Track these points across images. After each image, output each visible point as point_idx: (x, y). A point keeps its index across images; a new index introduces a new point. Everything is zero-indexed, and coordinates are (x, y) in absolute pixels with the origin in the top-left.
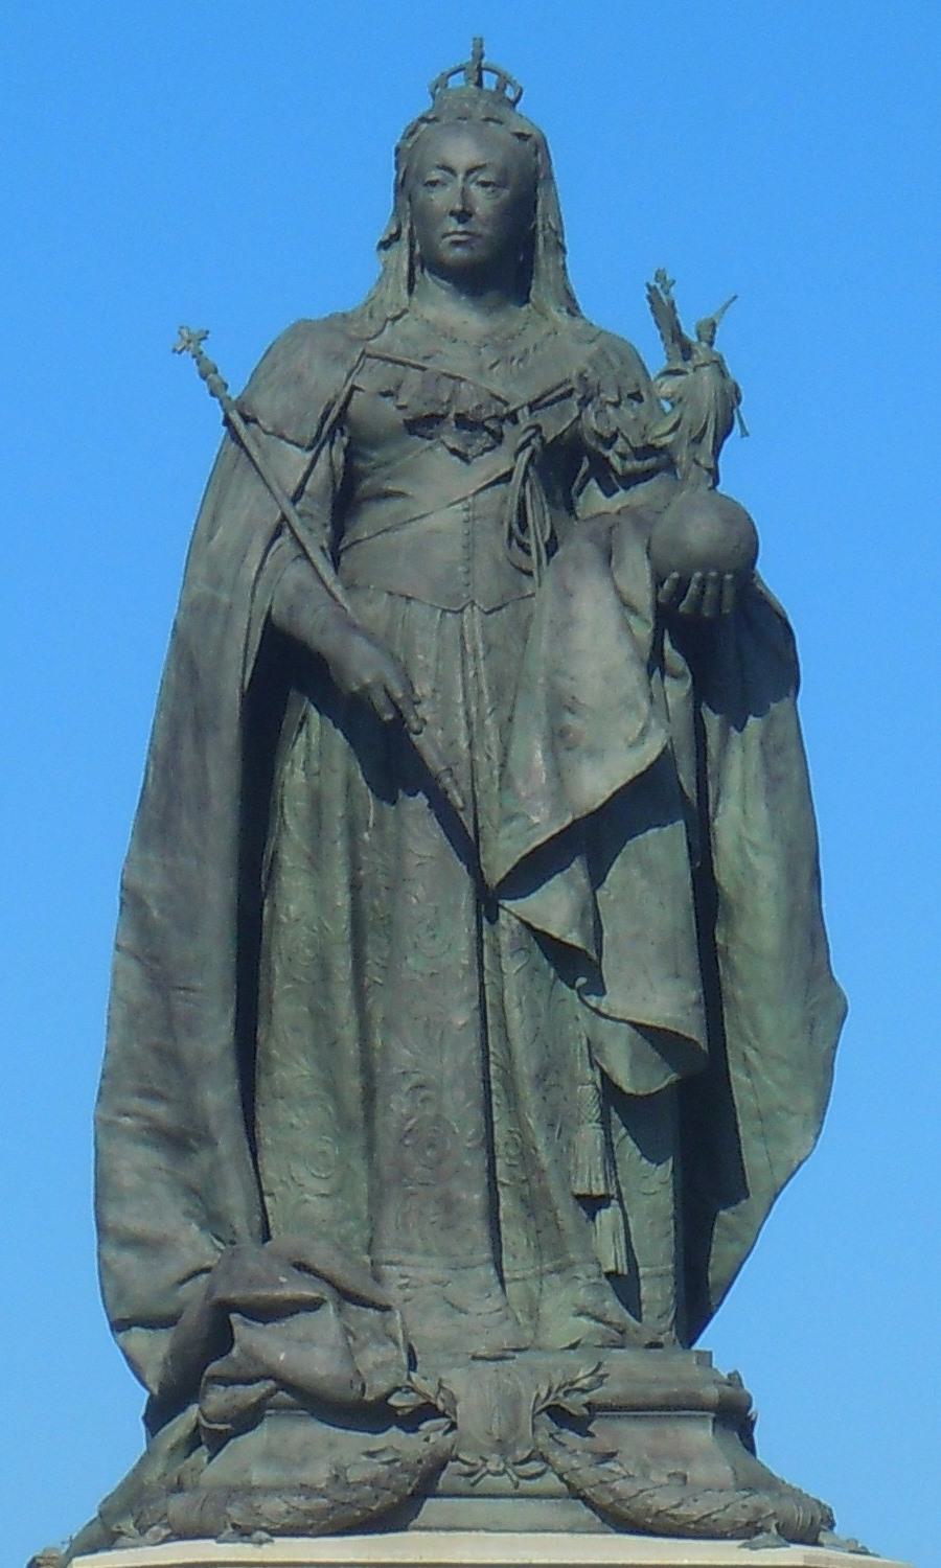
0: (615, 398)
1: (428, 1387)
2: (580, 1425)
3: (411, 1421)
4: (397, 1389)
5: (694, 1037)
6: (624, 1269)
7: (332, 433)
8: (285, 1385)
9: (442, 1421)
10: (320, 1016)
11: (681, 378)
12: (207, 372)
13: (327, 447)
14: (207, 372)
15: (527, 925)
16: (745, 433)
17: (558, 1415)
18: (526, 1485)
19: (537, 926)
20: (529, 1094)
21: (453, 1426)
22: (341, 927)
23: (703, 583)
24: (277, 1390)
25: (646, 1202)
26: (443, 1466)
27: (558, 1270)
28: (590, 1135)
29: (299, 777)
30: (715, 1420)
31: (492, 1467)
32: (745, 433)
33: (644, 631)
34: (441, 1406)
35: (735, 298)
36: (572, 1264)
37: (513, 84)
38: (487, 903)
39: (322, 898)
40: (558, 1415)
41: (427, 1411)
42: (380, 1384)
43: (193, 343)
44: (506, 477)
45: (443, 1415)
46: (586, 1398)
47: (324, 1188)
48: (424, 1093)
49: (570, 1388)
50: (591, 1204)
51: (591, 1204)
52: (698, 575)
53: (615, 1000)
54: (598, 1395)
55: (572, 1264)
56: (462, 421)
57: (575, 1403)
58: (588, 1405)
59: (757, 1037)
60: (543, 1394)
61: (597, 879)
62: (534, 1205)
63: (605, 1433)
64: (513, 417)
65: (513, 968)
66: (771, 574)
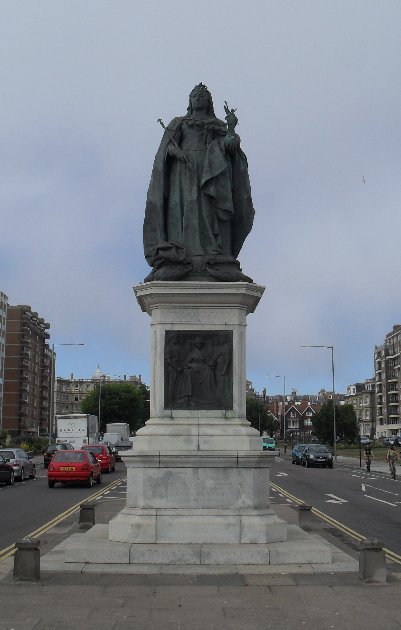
1: (189, 259)
9: (191, 265)
12: (162, 123)
14: (162, 123)
16: (238, 125)
27: (210, 244)
32: (238, 125)
33: (224, 153)
34: (191, 263)
35: (237, 109)
37: (206, 87)
38: (200, 189)
41: (189, 263)
42: (181, 259)
43: (159, 120)
45: (191, 264)
55: (212, 243)
56: (197, 125)
57: (212, 262)
60: (207, 261)
66: (243, 147)
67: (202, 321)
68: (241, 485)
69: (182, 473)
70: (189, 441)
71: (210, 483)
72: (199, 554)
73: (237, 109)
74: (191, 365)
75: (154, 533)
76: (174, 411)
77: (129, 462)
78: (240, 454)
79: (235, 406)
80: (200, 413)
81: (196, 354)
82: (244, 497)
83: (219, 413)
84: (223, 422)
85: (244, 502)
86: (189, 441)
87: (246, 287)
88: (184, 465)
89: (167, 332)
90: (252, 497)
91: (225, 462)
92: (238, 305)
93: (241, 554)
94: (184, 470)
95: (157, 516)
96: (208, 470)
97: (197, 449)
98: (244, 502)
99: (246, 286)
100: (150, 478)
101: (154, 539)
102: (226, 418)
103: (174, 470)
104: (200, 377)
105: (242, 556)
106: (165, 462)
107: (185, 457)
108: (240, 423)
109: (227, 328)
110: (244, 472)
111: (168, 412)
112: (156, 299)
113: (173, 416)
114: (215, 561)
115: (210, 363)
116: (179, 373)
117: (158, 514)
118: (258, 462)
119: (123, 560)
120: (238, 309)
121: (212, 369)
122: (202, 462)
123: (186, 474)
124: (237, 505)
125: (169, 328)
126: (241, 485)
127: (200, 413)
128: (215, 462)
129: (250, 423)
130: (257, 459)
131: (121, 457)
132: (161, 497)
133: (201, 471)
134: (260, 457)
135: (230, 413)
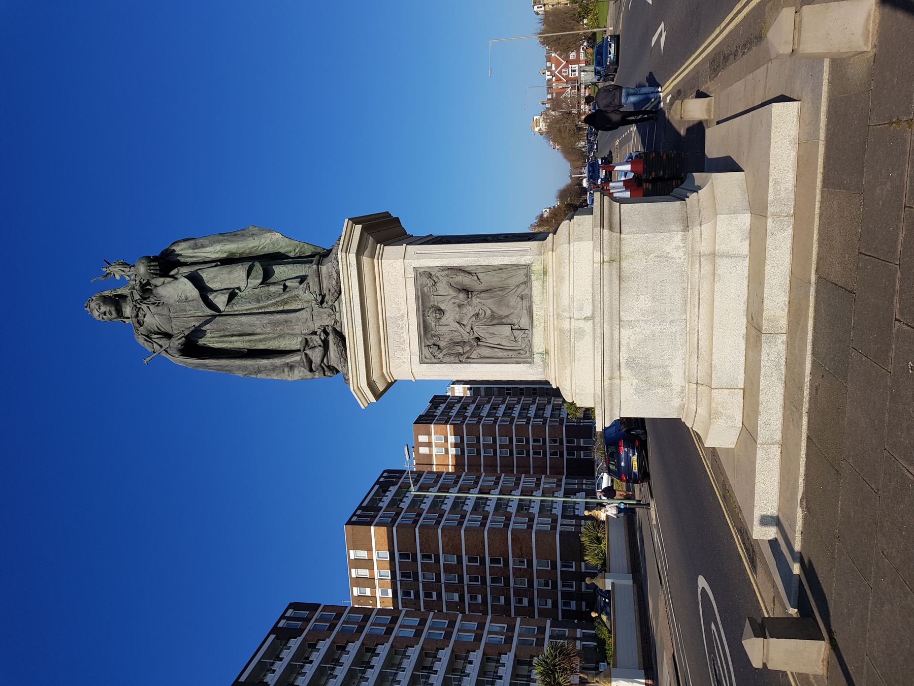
0: (134, 281)
2: (324, 297)
3: (327, 334)
4: (320, 338)
5: (248, 266)
6: (299, 280)
7: (150, 339)
8: (322, 361)
10: (260, 341)
11: (115, 274)
13: (153, 339)
15: (227, 306)
17: (322, 302)
18: (337, 310)
19: (226, 303)
20: (262, 304)
21: (328, 326)
22: (240, 338)
23: (150, 270)
24: (324, 363)
25: (290, 272)
26: (335, 328)
28: (272, 289)
29: (215, 344)
30: (321, 265)
31: (334, 318)
35: (105, 260)
36: (295, 295)
39: (236, 341)
40: (322, 302)
44: (148, 307)
45: (325, 328)
46: (318, 296)
47: (296, 338)
48: (265, 327)
49: (316, 299)
50: (285, 287)
51: (285, 287)
52: (149, 271)
53: (242, 285)
54: (318, 292)
57: (319, 299)
58: (320, 295)
59: (256, 247)
61: (212, 291)
62: (285, 302)
63: (325, 291)
64: (135, 306)
65: (237, 308)
67: (404, 312)
68: (647, 253)
69: (628, 344)
70: (580, 333)
71: (645, 302)
72: (769, 335)
73: (105, 260)
74: (468, 328)
75: (725, 391)
76: (535, 350)
77: (611, 416)
78: (598, 258)
79: (524, 260)
80: (537, 313)
81: (450, 318)
82: (667, 249)
83: (536, 285)
84: (550, 279)
85: (677, 248)
86: (580, 333)
87: (346, 253)
88: (617, 342)
89: (422, 362)
90: (668, 234)
91: (611, 281)
92: (376, 261)
93: (772, 267)
94: (623, 342)
95: (697, 383)
96: (624, 306)
97: (591, 321)
98: (678, 248)
99: (344, 254)
100: (637, 391)
101: (736, 391)
102: (545, 273)
103: (624, 355)
104: (483, 312)
105: (775, 265)
106: (612, 371)
107: (603, 343)
108: (550, 253)
109: (411, 274)
110: (626, 250)
111: (537, 358)
112: (375, 376)
113: (541, 350)
114: (783, 310)
115: (462, 296)
116: (479, 343)
117: (695, 382)
118: (611, 228)
119: (775, 455)
120: (381, 259)
121: (472, 295)
122: (611, 317)
123: (631, 338)
124: (682, 259)
125: (416, 359)
126: (647, 253)
127: (537, 313)
128: (611, 296)
129: (551, 235)
130: (606, 231)
131: (605, 427)
132: (668, 375)
133: (625, 317)
134: (602, 226)
135: (537, 267)
